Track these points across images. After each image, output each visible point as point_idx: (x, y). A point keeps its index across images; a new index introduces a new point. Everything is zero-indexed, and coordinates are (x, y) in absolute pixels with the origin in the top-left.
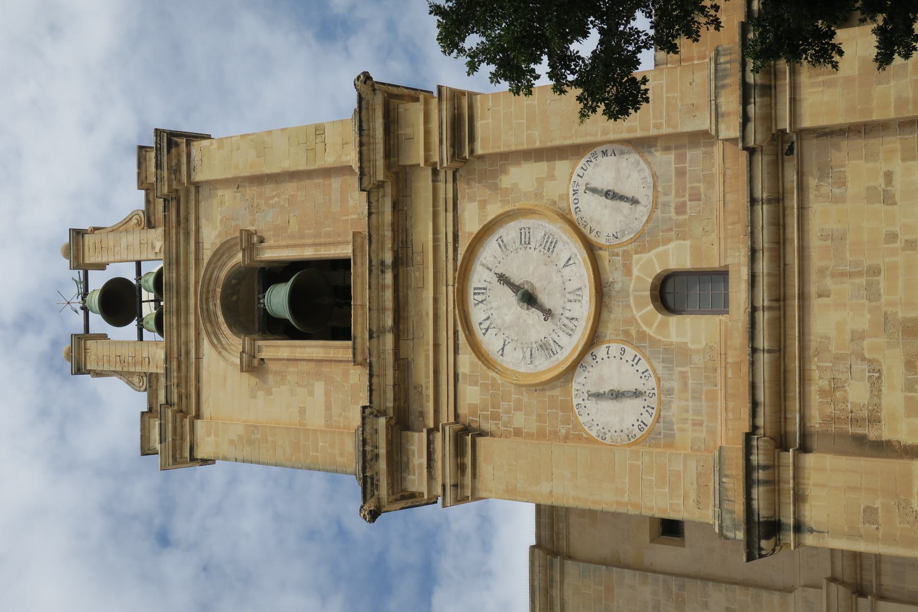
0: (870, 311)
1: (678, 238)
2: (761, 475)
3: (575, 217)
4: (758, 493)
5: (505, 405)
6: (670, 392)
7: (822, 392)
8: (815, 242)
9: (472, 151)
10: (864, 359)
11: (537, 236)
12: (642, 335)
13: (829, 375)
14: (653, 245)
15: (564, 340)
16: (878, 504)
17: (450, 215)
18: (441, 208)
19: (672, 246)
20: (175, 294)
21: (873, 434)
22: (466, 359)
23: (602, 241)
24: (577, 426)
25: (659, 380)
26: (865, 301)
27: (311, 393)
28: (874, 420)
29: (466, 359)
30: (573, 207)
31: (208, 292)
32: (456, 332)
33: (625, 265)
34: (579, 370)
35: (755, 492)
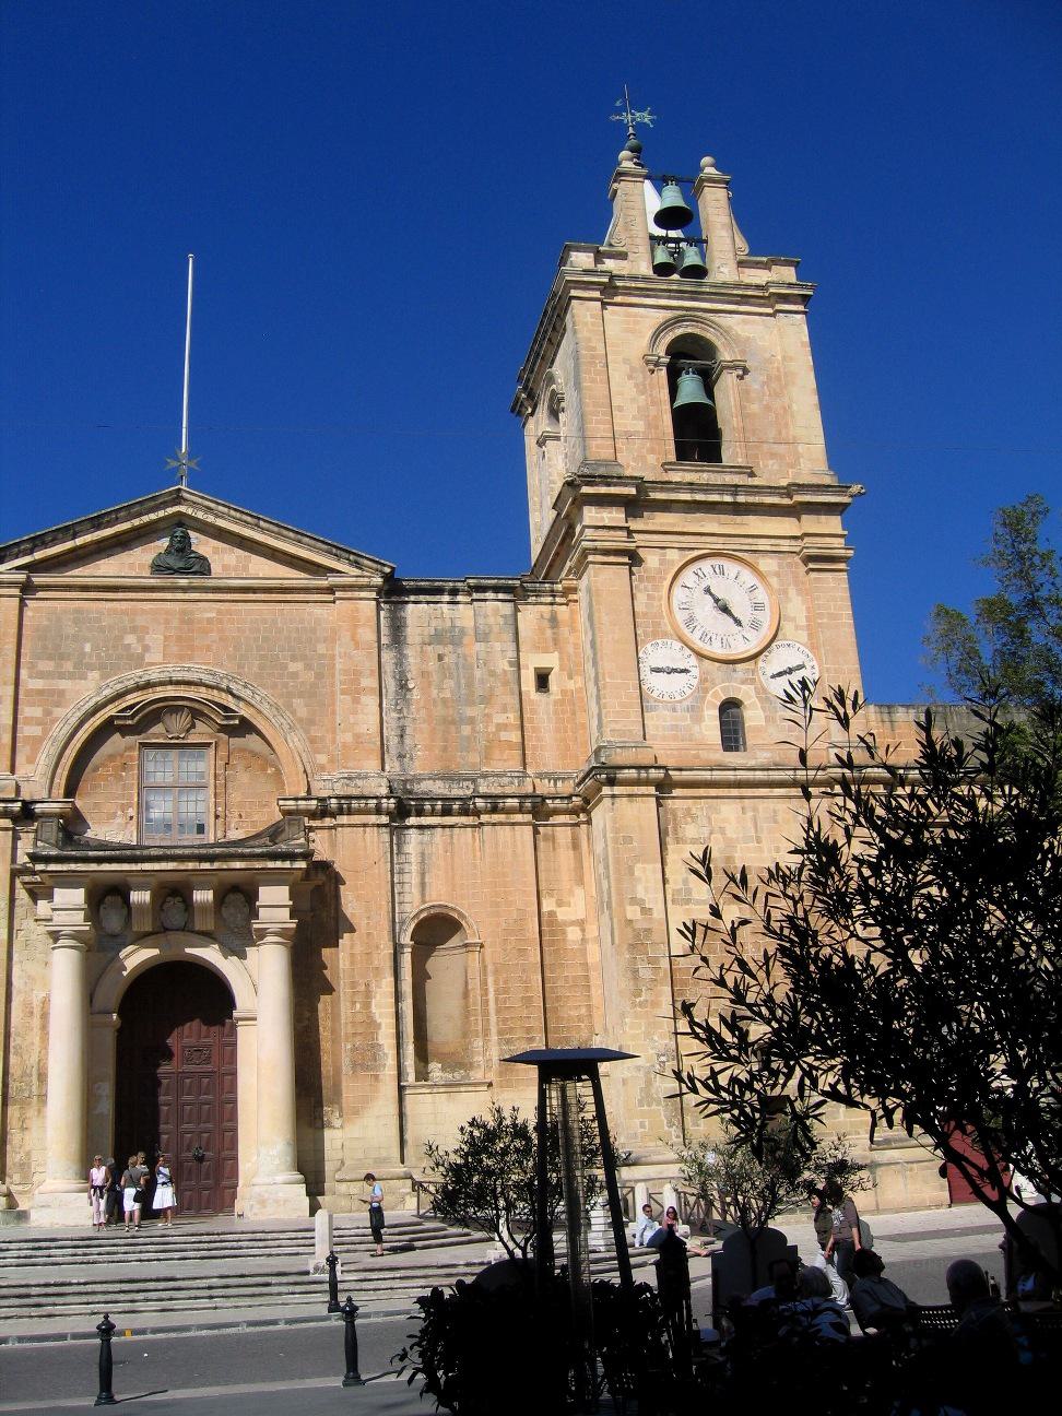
0: (738, 838)
1: (766, 717)
2: (643, 774)
3: (774, 645)
4: (633, 773)
5: (650, 586)
6: (674, 710)
7: (689, 810)
8: (771, 804)
9: (813, 570)
10: (711, 833)
11: (759, 615)
12: (706, 691)
13: (699, 813)
14: (760, 699)
15: (698, 634)
16: (635, 844)
17: (769, 548)
18: (773, 541)
19: (760, 713)
20: (693, 289)
21: (669, 839)
22: (673, 555)
23: (760, 664)
24: (645, 642)
25: (680, 702)
26: (741, 835)
27: (634, 418)
28: (678, 841)
29: (676, 558)
31: (697, 322)
32: (693, 549)
33: (747, 679)
34: (680, 644)
35: (634, 771)
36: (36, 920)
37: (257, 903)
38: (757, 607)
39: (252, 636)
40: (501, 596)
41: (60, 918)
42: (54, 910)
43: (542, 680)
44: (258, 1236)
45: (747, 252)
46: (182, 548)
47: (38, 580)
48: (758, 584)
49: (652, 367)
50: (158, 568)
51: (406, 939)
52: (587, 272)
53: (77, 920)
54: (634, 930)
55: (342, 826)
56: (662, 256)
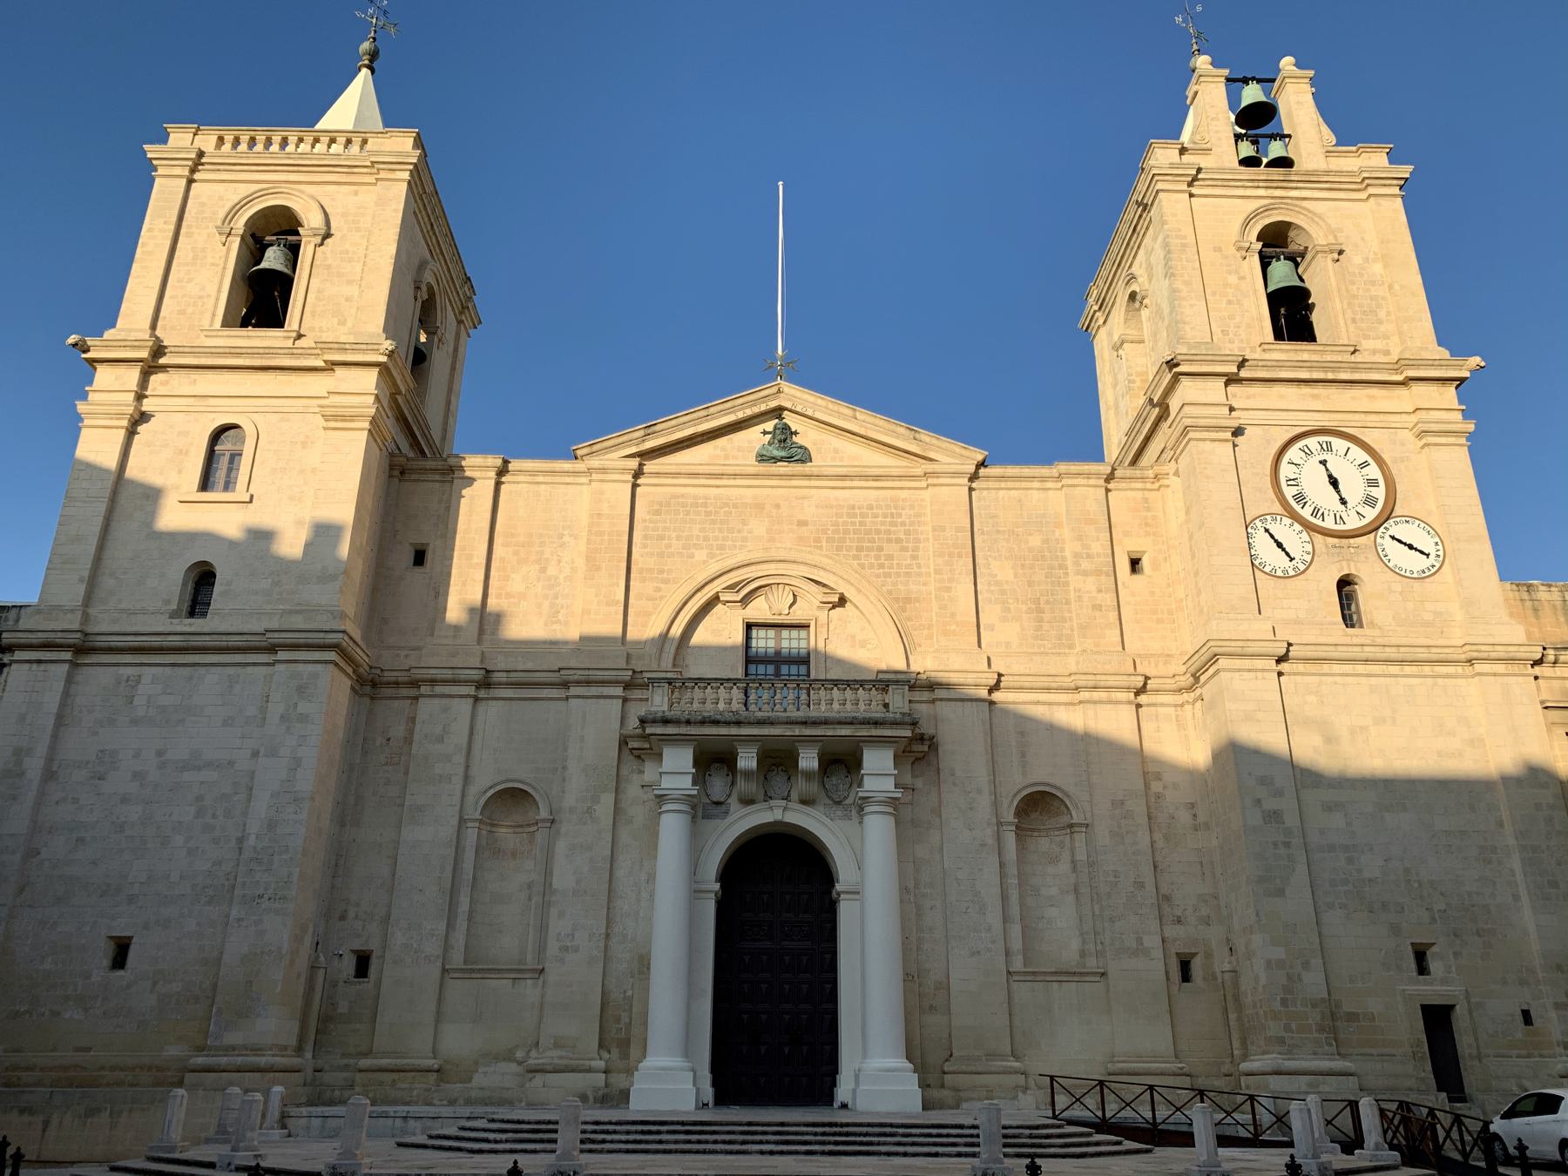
3: (1391, 521)
30: (1398, 519)
36: (643, 786)
37: (862, 772)
38: (1372, 483)
39: (849, 520)
40: (1092, 482)
41: (667, 783)
42: (661, 773)
43: (1135, 564)
44: (888, 1130)
45: (1334, 143)
46: (784, 435)
47: (650, 466)
48: (1370, 460)
49: (1244, 253)
50: (762, 458)
51: (1009, 816)
52: (1172, 166)
53: (685, 783)
54: (1263, 812)
55: (941, 700)
56: (1247, 149)
